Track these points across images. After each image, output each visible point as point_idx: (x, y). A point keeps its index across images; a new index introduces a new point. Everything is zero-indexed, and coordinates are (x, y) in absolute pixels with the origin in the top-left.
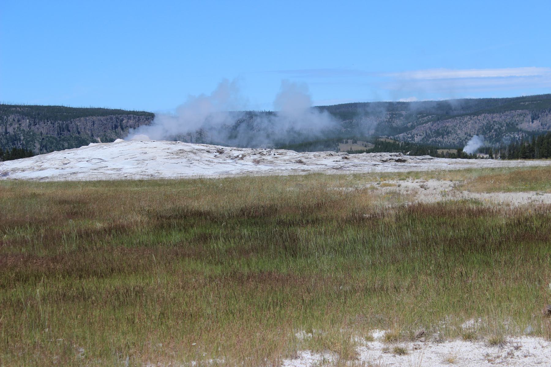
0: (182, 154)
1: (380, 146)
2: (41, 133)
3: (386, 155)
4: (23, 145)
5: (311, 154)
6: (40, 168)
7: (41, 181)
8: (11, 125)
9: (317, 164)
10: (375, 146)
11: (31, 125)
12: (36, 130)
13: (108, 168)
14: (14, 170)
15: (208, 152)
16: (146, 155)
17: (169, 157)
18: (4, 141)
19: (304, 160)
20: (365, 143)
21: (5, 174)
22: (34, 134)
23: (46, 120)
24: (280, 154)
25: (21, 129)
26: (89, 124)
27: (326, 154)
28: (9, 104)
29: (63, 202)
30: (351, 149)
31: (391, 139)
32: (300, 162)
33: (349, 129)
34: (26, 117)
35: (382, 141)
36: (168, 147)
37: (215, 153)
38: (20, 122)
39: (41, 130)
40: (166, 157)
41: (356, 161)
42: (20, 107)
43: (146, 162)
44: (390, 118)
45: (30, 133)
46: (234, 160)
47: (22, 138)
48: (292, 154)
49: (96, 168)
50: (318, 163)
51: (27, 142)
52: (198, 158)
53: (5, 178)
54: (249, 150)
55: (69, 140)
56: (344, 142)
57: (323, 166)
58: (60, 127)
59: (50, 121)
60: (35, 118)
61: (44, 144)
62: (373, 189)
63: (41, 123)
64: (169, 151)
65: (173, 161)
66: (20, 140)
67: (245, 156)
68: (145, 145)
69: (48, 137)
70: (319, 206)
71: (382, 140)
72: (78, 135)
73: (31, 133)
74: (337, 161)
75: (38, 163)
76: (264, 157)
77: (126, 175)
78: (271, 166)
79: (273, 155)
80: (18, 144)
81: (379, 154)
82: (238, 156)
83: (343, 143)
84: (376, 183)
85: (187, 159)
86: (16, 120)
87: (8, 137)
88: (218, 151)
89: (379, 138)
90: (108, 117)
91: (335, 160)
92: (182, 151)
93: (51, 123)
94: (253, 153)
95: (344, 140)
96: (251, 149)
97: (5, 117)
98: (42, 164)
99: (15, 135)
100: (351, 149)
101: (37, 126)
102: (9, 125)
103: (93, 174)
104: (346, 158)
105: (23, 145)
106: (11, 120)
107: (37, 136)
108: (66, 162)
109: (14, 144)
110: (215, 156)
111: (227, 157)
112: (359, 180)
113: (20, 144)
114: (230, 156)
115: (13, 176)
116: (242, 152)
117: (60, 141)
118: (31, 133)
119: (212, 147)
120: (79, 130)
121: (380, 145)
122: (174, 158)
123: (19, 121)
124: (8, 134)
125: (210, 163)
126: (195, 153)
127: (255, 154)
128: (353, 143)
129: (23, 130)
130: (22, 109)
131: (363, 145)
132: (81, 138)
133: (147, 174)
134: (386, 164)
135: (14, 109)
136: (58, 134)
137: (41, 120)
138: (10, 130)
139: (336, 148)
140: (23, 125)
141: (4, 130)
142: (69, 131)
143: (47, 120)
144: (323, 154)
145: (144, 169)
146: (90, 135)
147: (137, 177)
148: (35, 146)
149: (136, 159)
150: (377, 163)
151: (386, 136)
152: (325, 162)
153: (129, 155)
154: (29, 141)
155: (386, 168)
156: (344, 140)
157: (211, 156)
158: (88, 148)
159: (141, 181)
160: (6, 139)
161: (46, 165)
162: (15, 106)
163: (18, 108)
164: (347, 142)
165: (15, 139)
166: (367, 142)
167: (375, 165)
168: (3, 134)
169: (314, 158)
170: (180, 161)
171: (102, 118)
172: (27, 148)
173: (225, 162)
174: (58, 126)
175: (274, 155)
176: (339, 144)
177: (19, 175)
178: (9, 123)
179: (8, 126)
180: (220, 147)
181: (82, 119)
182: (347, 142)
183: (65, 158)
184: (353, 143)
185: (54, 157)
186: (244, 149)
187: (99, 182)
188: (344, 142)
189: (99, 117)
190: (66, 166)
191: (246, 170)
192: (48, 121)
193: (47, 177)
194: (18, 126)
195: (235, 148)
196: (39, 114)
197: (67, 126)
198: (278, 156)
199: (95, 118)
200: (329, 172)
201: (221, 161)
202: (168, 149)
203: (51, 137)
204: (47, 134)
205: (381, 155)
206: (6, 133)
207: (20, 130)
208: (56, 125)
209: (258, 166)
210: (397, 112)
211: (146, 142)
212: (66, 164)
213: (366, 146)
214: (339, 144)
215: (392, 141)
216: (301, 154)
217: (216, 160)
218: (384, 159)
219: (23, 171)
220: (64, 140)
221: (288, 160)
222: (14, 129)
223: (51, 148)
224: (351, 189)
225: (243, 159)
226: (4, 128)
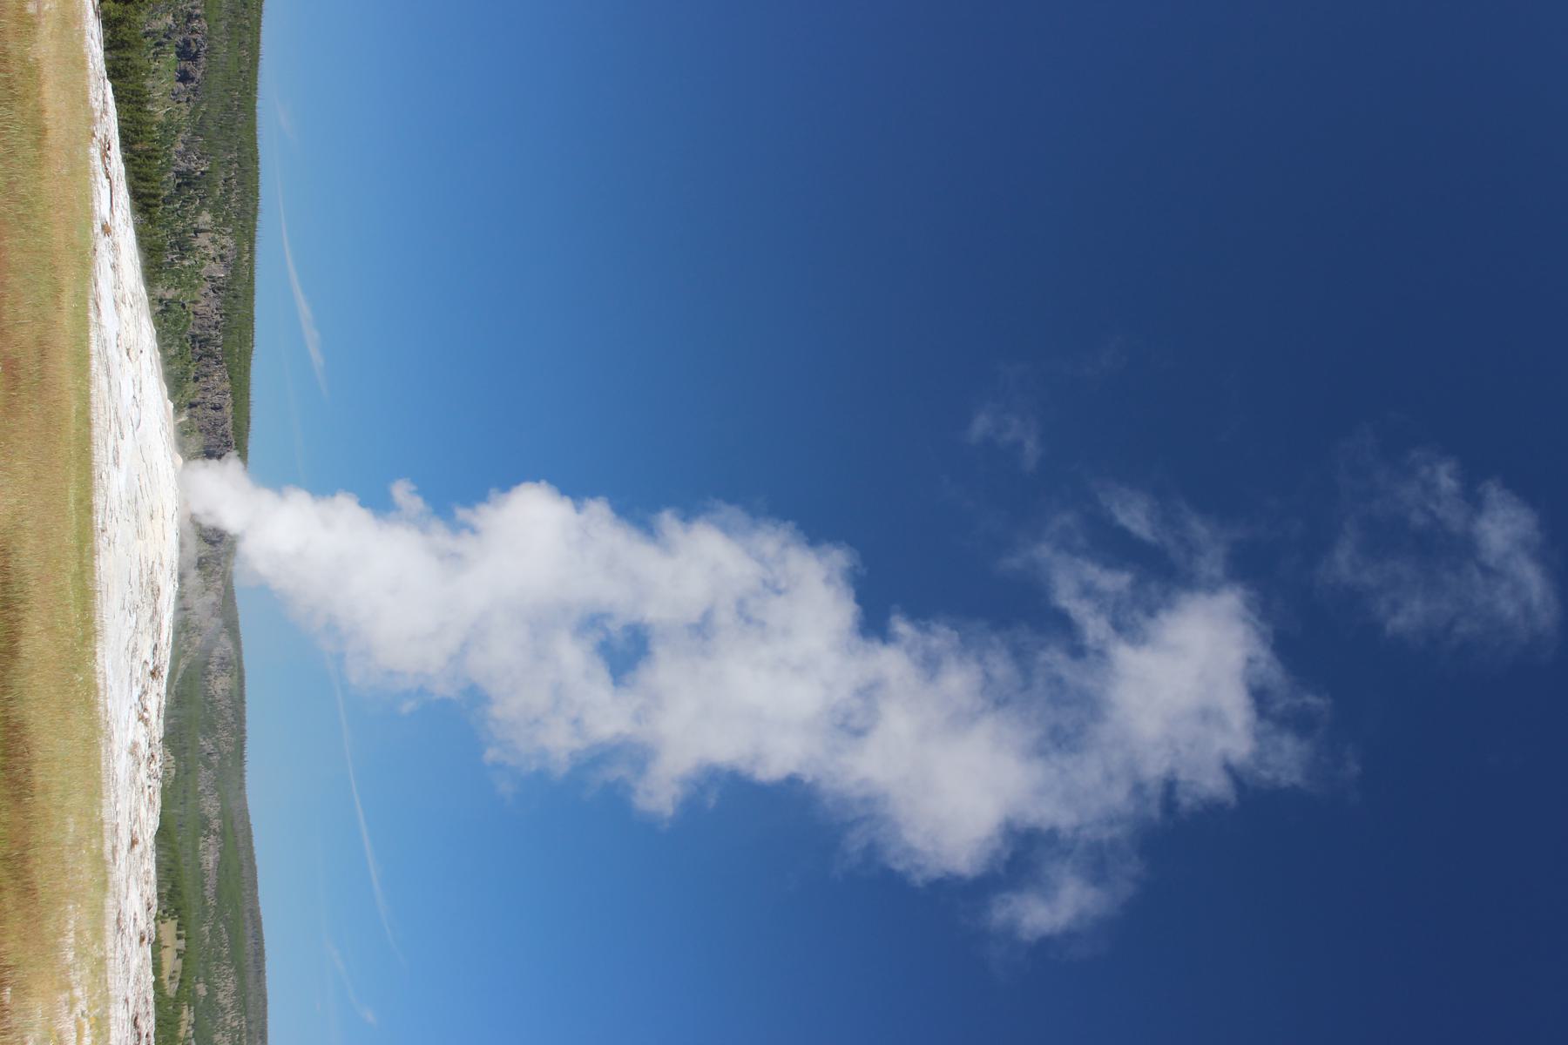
0: (150, 593)
1: (171, 1008)
2: (195, 302)
3: (148, 1025)
4: (172, 263)
5: (150, 865)
6: (119, 300)
7: (91, 305)
8: (214, 241)
9: (128, 878)
10: (171, 999)
11: (214, 281)
12: (203, 292)
13: (120, 440)
14: (115, 248)
15: (156, 647)
16: (148, 519)
17: (144, 566)
18: (179, 226)
19: (138, 849)
20: (178, 978)
21: (106, 230)
22: (193, 287)
23: (223, 311)
24: (150, 799)
25: (207, 262)
26: (216, 400)
27: (150, 897)
28: (257, 239)
29: (43, 349)
30: (166, 947)
31: (187, 1031)
32: (134, 843)
33: (208, 940)
34: (229, 273)
35: (182, 1013)
36: (165, 564)
37: (152, 662)
38: (218, 260)
39: (204, 302)
40: (143, 561)
41: (135, 962)
42: (251, 261)
43: (133, 519)
44: (232, 1028)
45: (197, 278)
46: (136, 700)
47: (186, 263)
48: (150, 823)
49: (119, 415)
50: (132, 881)
51: (177, 274)
52: (141, 626)
53: (98, 228)
54: (159, 733)
55: (181, 358)
56: (179, 932)
57: (125, 891)
58: (207, 340)
59: (217, 318)
60: (228, 290)
61: (175, 307)
62: (72, 1003)
63: (218, 302)
64: (156, 566)
65: (135, 574)
66: (183, 258)
67: (146, 725)
68: (168, 516)
69: (188, 314)
70: (28, 891)
71: (185, 1012)
72: (193, 375)
73: (197, 282)
74: (135, 920)
75: (131, 298)
76: (144, 764)
77: (104, 476)
78: (125, 781)
79: (149, 783)
80: (174, 254)
81: (151, 1008)
82: (145, 710)
83: (178, 929)
84: (84, 1009)
85: (140, 604)
86: (223, 252)
87: (187, 235)
88: (156, 668)
89: (189, 1006)
90: (232, 438)
91: (139, 917)
92: (156, 593)
93: (217, 323)
94: (153, 742)
95: (183, 932)
96: (162, 736)
97: (230, 230)
98: (128, 306)
99: (191, 249)
100: (166, 947)
101: (212, 294)
102: (213, 238)
103: (107, 409)
104: (142, 939)
105: (172, 263)
106: (224, 242)
107: (189, 292)
108: (132, 354)
109: (172, 246)
110: (146, 662)
111: (143, 686)
112: (92, 971)
113: (172, 260)
114: (145, 693)
115: (103, 243)
116: (154, 719)
117: (181, 339)
118: (197, 282)
119: (166, 655)
120: (205, 379)
121: (174, 1007)
122: (141, 575)
123: (222, 257)
124: (193, 234)
125: (131, 650)
126: (152, 619)
127: (149, 747)
128: (177, 950)
129: (202, 266)
130: (246, 264)
131: (174, 972)
132: (187, 382)
133: (108, 521)
134: (129, 1026)
135: (247, 248)
136: (194, 337)
137: (225, 302)
138: (203, 239)
139: (167, 915)
140: (213, 265)
141: (203, 227)
142: (200, 359)
143: (225, 314)
144: (151, 890)
145: (117, 514)
146: (192, 400)
147: (98, 501)
148: (168, 288)
149: (140, 500)
150: (131, 1007)
151: (193, 1020)
152: (134, 895)
153: (148, 484)
154: (179, 277)
155: (121, 1025)
156: (183, 932)
157: (147, 655)
158: (163, 399)
159: (90, 509)
160: (184, 231)
161: (126, 312)
162: (251, 250)
163: (248, 255)
164: (179, 937)
165: (183, 248)
166: (181, 981)
167: (126, 1001)
168: (195, 226)
169: (142, 871)
170: (136, 587)
171: (229, 426)
172: (164, 272)
173: (134, 683)
174: (211, 335)
175: (149, 787)
176: (176, 921)
177: (104, 259)
178: (217, 237)
179: (211, 235)
180: (166, 672)
181: (227, 385)
182: (179, 937)
183: (141, 352)
184: (177, 950)
185: (144, 330)
186: (161, 721)
187: (88, 423)
188: (179, 932)
189: (230, 420)
190: (125, 354)
191: (117, 727)
192: (221, 317)
193: (99, 315)
194: (212, 256)
195: (163, 703)
196: (235, 297)
197: (211, 355)
198: (147, 794)
199: (229, 410)
200: (110, 902)
201: (134, 675)
202: (161, 564)
203: (188, 321)
204: (195, 313)
205: (148, 1013)
206: (197, 231)
207: (203, 259)
208: (213, 333)
209: (125, 753)
210: (245, 1041)
211: (175, 519)
212: (128, 354)
213: (171, 978)
214: (176, 921)
215: (182, 1033)
216: (150, 842)
217: (137, 664)
218: (142, 1023)
219: (113, 267)
220: (181, 346)
221: (138, 816)
222: (205, 247)
223: (166, 321)
224: (71, 956)
225: (139, 720)
226: (207, 227)
